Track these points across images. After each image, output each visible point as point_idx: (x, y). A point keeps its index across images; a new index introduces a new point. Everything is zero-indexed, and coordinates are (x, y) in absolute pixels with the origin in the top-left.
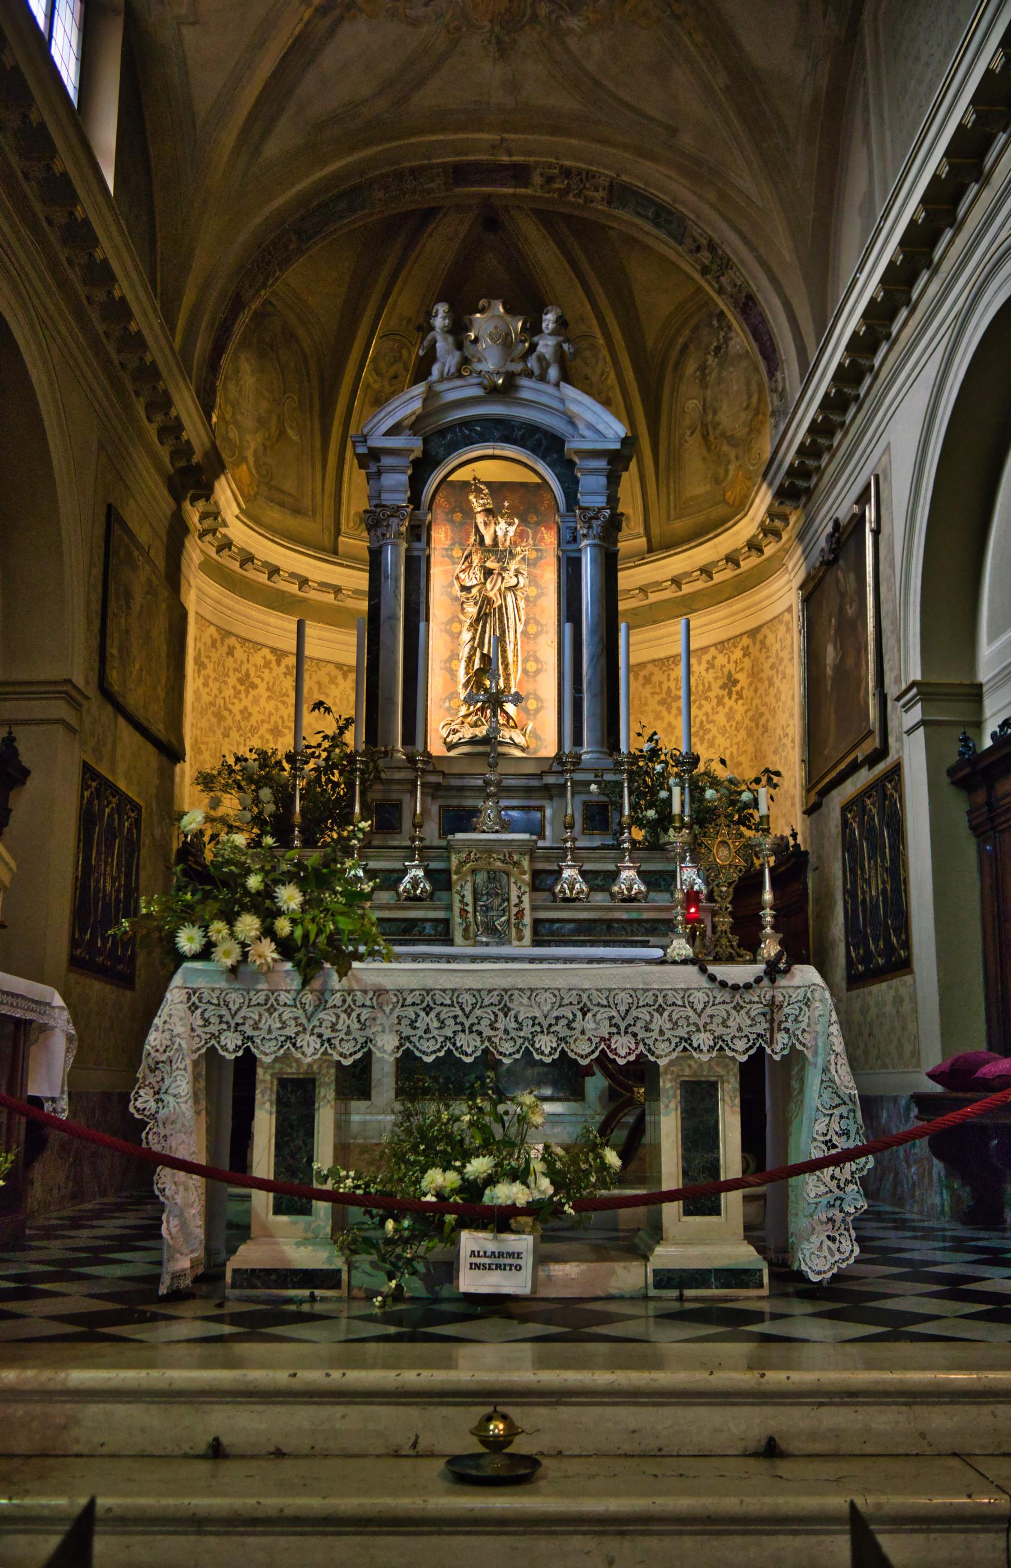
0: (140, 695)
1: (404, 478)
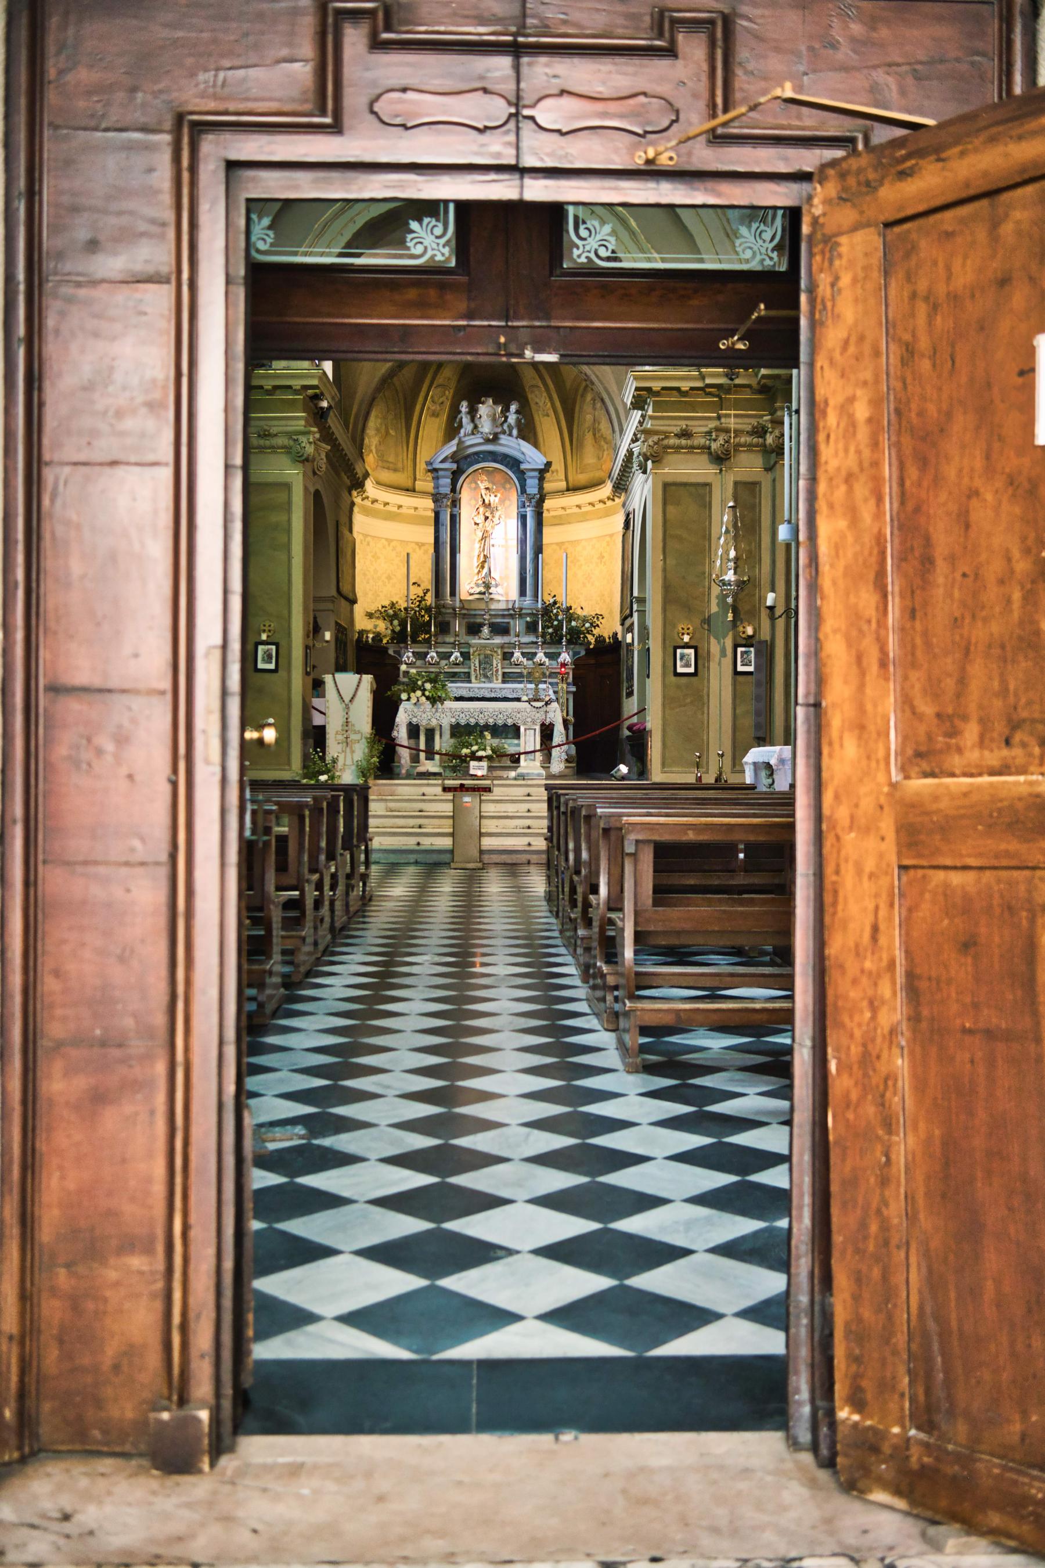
0: (345, 589)
1: (449, 481)
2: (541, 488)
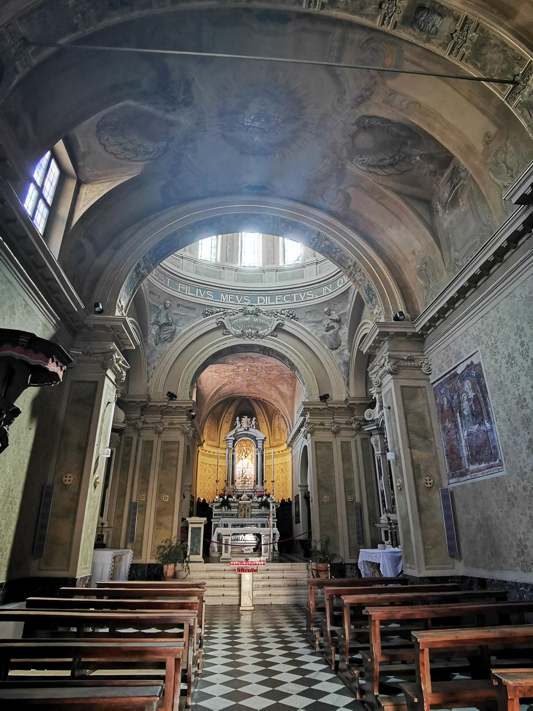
2: (263, 446)
